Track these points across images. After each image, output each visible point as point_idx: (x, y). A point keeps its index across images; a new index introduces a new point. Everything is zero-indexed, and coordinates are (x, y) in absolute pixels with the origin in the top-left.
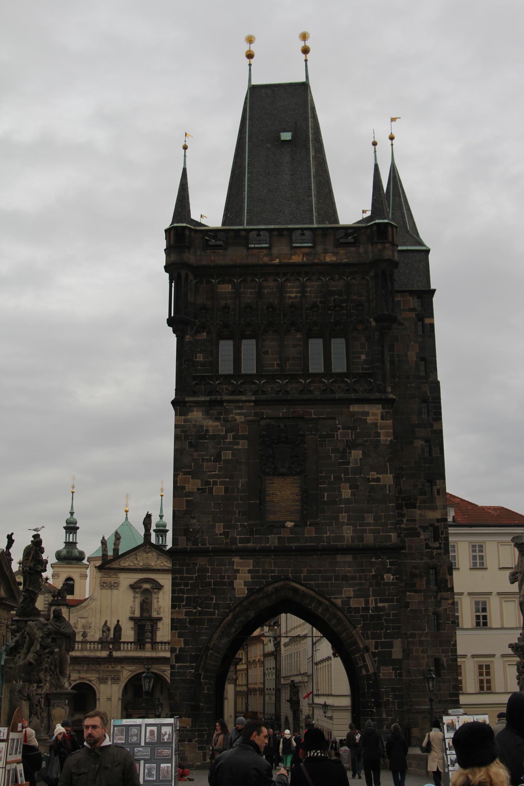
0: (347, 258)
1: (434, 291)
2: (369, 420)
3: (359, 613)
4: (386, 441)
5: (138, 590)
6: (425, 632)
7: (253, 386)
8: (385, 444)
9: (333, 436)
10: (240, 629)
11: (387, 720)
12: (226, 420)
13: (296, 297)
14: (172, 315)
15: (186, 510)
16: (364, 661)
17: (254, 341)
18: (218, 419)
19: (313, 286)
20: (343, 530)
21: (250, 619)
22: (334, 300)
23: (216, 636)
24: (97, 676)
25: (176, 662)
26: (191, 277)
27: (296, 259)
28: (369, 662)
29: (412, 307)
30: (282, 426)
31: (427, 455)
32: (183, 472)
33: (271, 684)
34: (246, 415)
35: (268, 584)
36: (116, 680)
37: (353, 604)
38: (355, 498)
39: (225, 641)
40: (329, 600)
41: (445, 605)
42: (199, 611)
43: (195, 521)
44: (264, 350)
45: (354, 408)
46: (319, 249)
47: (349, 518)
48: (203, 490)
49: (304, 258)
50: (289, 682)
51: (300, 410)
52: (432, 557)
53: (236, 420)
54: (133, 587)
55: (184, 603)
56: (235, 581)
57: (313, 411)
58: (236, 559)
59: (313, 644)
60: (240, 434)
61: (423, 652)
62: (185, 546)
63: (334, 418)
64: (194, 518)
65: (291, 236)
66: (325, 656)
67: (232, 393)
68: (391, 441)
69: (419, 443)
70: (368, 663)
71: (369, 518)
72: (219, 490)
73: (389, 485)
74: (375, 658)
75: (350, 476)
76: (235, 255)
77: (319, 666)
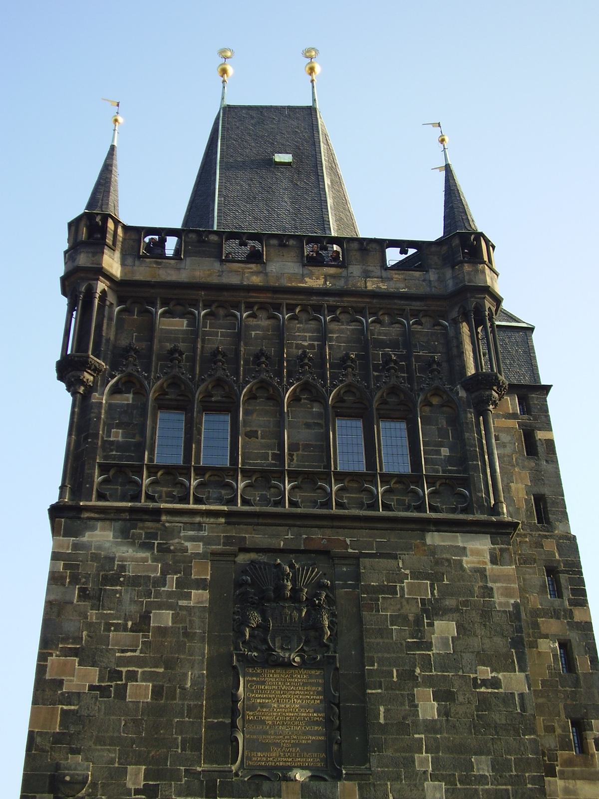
0: (406, 287)
2: (467, 563)
7: (223, 492)
8: (505, 612)
12: (164, 549)
13: (311, 347)
18: (146, 546)
19: (341, 333)
20: (423, 790)
34: (207, 541)
38: (447, 720)
44: (248, 429)
45: (434, 539)
46: (355, 270)
48: (103, 691)
49: (328, 283)
51: (320, 536)
53: (186, 550)
57: (349, 541)
60: (193, 577)
63: (395, 557)
68: (516, 605)
72: (140, 692)
75: (434, 673)
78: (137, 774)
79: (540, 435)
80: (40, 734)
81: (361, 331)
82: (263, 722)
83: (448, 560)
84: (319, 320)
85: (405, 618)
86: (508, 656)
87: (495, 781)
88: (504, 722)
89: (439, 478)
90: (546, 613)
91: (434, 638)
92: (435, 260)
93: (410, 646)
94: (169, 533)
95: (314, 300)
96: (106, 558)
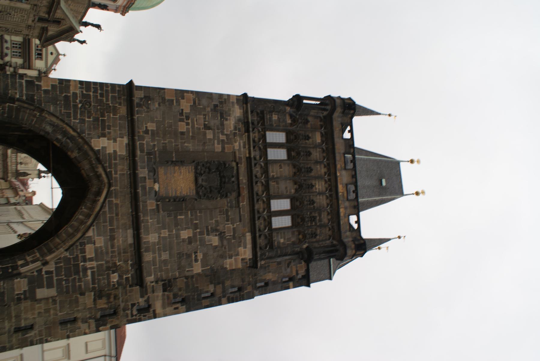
1: (308, 285)
3: (81, 253)
6: (58, 312)
9: (228, 220)
10: (58, 145)
12: (235, 134)
13: (316, 189)
15: (165, 99)
16: (33, 262)
18: (235, 128)
19: (322, 201)
21: (69, 153)
22: (316, 217)
23: (54, 119)
25: (26, 81)
27: (341, 188)
28: (31, 266)
29: (299, 272)
30: (233, 179)
31: (203, 295)
32: (195, 99)
34: (239, 150)
35: (105, 169)
37: (89, 248)
38: (181, 242)
39: (49, 129)
40: (92, 225)
41: (84, 326)
42: (77, 105)
43: (157, 106)
44: (282, 165)
45: (249, 236)
46: (347, 204)
47: (164, 238)
48: (181, 114)
51: (245, 193)
52: (124, 310)
53: (235, 142)
55: (84, 92)
56: (106, 139)
57: (245, 203)
58: (125, 140)
59: (22, 222)
60: (226, 146)
61: (39, 313)
62: (136, 96)
63: (240, 221)
64: (159, 105)
67: (254, 141)
68: (226, 268)
69: (211, 288)
71: (165, 256)
72: (182, 127)
73: (192, 270)
74: (37, 271)
75: (198, 237)
77: (7, 227)
79: (291, 284)
80: (165, 92)
81: (324, 208)
82: (175, 173)
83: (241, 242)
84: (326, 191)
85: (218, 226)
86: (207, 266)
88: (182, 264)
89: (272, 238)
92: (354, 234)
93: (207, 227)
94: (241, 136)
95: (334, 189)
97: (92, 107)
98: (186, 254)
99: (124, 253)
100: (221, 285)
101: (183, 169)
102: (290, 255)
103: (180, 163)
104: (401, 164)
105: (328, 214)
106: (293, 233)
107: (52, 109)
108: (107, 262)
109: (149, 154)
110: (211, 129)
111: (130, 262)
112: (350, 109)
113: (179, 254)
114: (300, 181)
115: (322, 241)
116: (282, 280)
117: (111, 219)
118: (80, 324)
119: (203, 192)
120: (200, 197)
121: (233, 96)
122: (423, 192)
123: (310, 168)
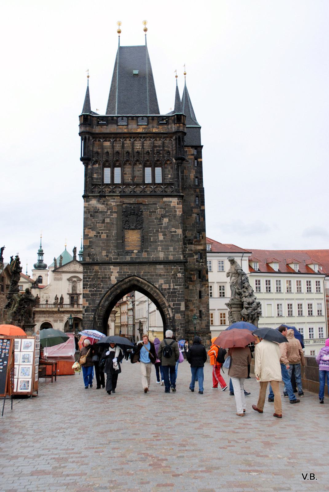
0: (163, 130)
1: (202, 146)
3: (166, 290)
4: (179, 214)
5: (70, 281)
9: (155, 212)
11: (178, 337)
12: (107, 205)
13: (139, 148)
14: (82, 156)
16: (168, 311)
17: (120, 168)
18: (103, 204)
19: (148, 143)
22: (157, 150)
23: (103, 301)
24: (53, 319)
25: (85, 312)
26: (91, 138)
27: (139, 130)
30: (132, 207)
33: (131, 322)
34: (116, 202)
36: (61, 321)
39: (107, 303)
40: (153, 285)
43: (93, 250)
45: (165, 199)
46: (150, 126)
47: (162, 249)
48: (97, 236)
50: (138, 321)
51: (140, 200)
54: (69, 280)
57: (146, 200)
58: (112, 267)
63: (156, 204)
64: (92, 249)
65: (137, 120)
66: (153, 310)
69: (194, 215)
70: (170, 312)
71: (171, 249)
72: (104, 236)
76: (112, 129)
77: (151, 314)
78: (104, 253)
82: (128, 241)
85: (158, 218)
87: (174, 252)
90: (194, 208)
91: (164, 223)
94: (108, 201)
95: (140, 135)
96: (95, 207)
97: (96, 283)
98: (171, 237)
99: (168, 270)
100: (193, 209)
101: (127, 237)
102: (178, 172)
103: (123, 238)
104: (120, 46)
105: (156, 140)
106: (166, 168)
107: (98, 302)
108: (171, 278)
109: (118, 255)
110: (104, 219)
111: (173, 267)
112: (87, 119)
113: (171, 242)
114: (134, 161)
115: (172, 146)
116: (196, 167)
117: (151, 275)
118: (203, 289)
119: (139, 225)
120: (141, 228)
121: (84, 204)
122: (145, 23)
123: (126, 153)
